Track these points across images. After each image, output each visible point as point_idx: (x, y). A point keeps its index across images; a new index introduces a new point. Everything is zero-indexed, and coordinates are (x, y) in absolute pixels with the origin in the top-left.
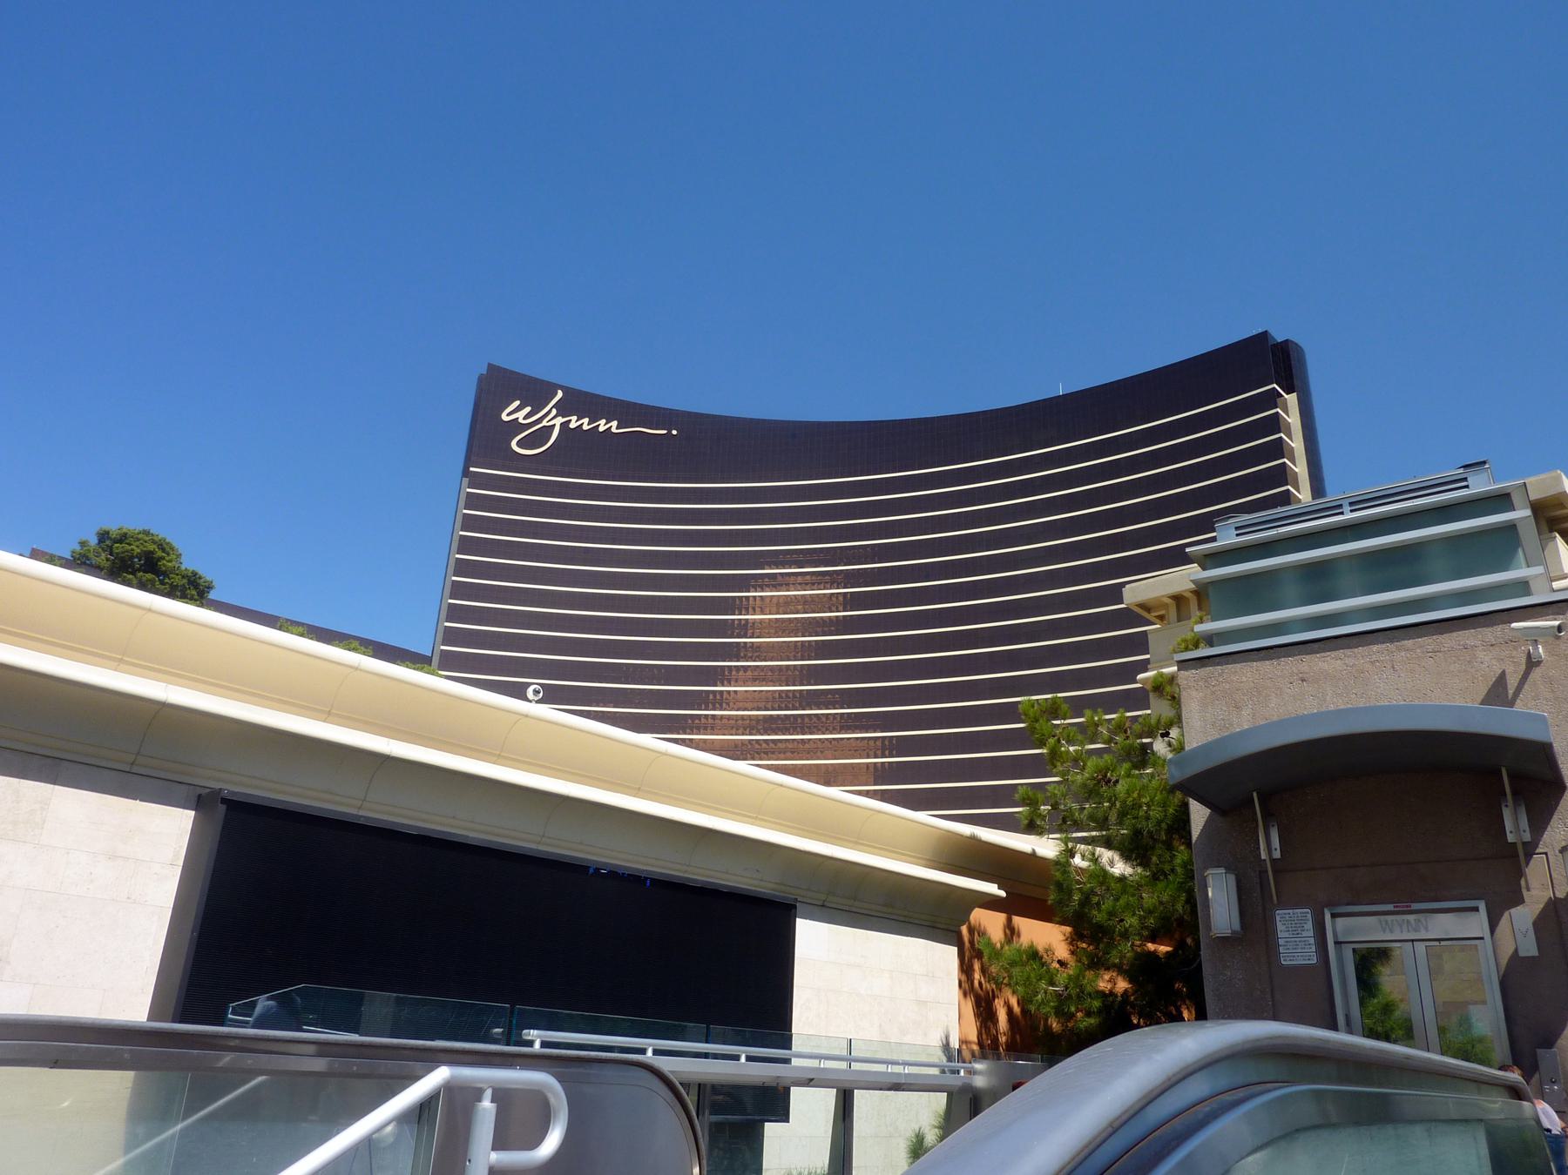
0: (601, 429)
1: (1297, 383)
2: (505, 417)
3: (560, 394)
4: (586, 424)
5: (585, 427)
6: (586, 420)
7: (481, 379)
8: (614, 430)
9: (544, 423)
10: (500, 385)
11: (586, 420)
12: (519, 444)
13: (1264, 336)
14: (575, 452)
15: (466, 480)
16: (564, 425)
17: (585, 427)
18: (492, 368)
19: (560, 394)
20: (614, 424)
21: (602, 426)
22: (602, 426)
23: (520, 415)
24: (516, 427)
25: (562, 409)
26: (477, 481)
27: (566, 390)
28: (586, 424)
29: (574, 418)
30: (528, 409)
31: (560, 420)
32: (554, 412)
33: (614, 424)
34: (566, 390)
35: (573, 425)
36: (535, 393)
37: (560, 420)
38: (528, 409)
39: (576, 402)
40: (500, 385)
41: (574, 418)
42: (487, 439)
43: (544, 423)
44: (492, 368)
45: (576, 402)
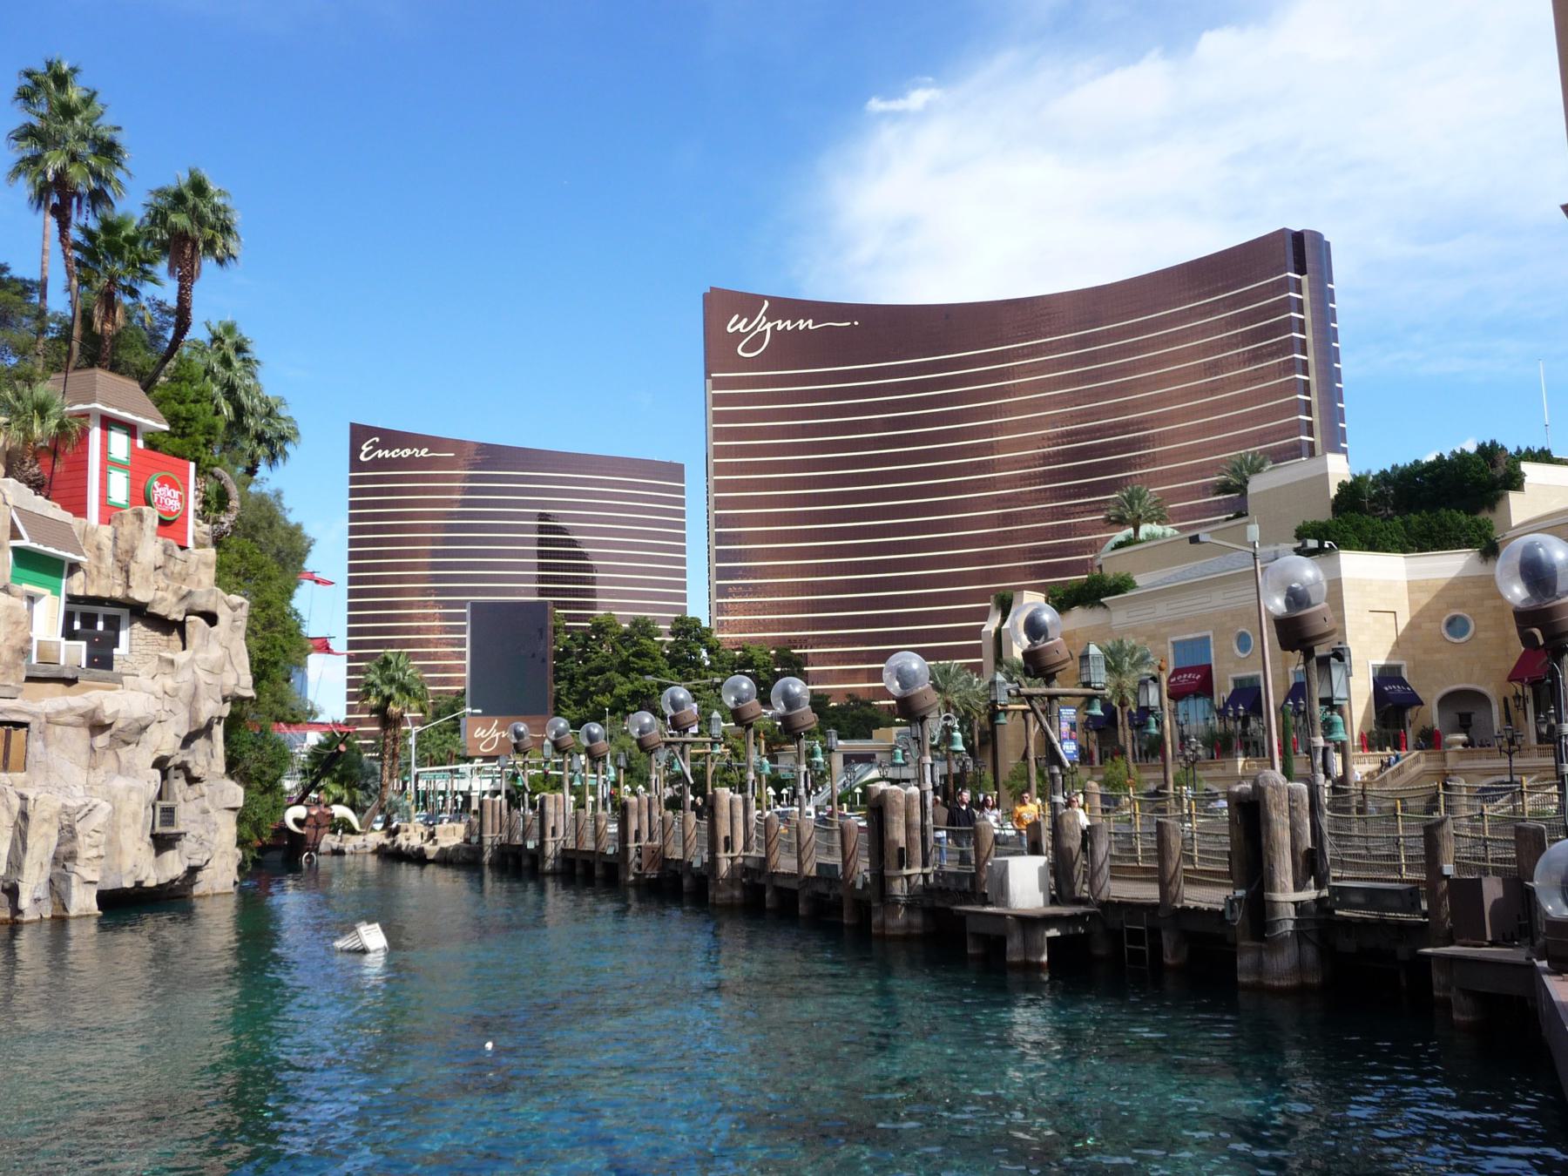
2: (730, 330)
4: (789, 325)
7: (705, 296)
10: (720, 305)
13: (1284, 231)
14: (786, 349)
15: (709, 382)
20: (810, 322)
21: (801, 324)
22: (801, 324)
23: (740, 326)
24: (739, 336)
25: (771, 316)
26: (718, 384)
27: (771, 299)
28: (789, 325)
31: (769, 326)
33: (810, 322)
37: (769, 326)
39: (784, 307)
40: (720, 305)
42: (719, 351)
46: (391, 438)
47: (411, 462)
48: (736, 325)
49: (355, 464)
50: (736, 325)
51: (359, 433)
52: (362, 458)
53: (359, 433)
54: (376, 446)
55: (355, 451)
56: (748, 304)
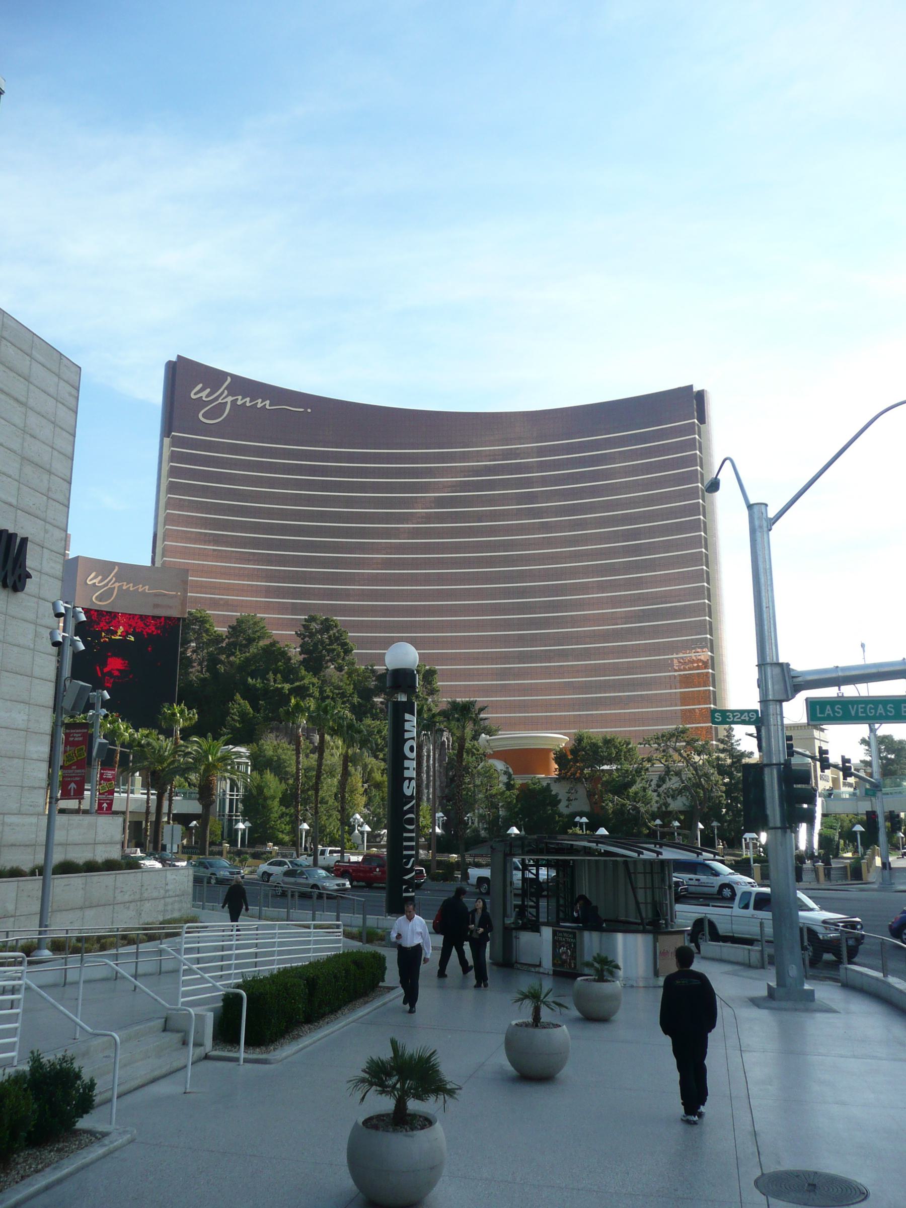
0: (259, 406)
3: (229, 379)
5: (248, 404)
6: (248, 399)
8: (267, 407)
9: (220, 401)
11: (248, 399)
15: (167, 441)
16: (234, 402)
17: (248, 404)
18: (179, 356)
19: (229, 379)
20: (268, 402)
23: (203, 394)
24: (201, 403)
25: (232, 390)
27: (234, 377)
29: (240, 397)
30: (208, 390)
31: (230, 399)
32: (226, 392)
33: (268, 402)
35: (239, 403)
37: (230, 399)
38: (208, 390)
41: (240, 397)
43: (220, 401)
44: (179, 356)
48: (199, 392)
50: (199, 392)
56: (213, 377)
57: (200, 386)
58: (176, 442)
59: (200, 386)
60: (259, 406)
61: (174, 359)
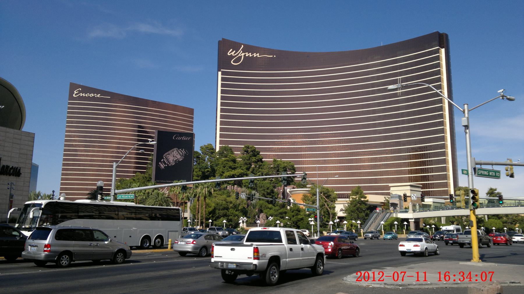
0: (255, 56)
1: (445, 44)
2: (229, 54)
3: (243, 46)
5: (250, 56)
12: (233, 62)
14: (248, 63)
15: (220, 73)
16: (245, 55)
17: (250, 56)
18: (223, 39)
19: (243, 46)
20: (258, 54)
23: (233, 53)
24: (232, 57)
31: (243, 54)
33: (258, 54)
34: (244, 45)
35: (247, 55)
36: (236, 46)
37: (243, 54)
39: (248, 48)
45: (248, 48)
46: (86, 89)
47: (94, 99)
48: (231, 53)
49: (71, 97)
50: (231, 53)
51: (73, 87)
52: (74, 96)
53: (73, 87)
54: (80, 92)
55: (71, 93)
57: (231, 50)
58: (223, 74)
59: (231, 50)
60: (255, 56)
61: (221, 39)
